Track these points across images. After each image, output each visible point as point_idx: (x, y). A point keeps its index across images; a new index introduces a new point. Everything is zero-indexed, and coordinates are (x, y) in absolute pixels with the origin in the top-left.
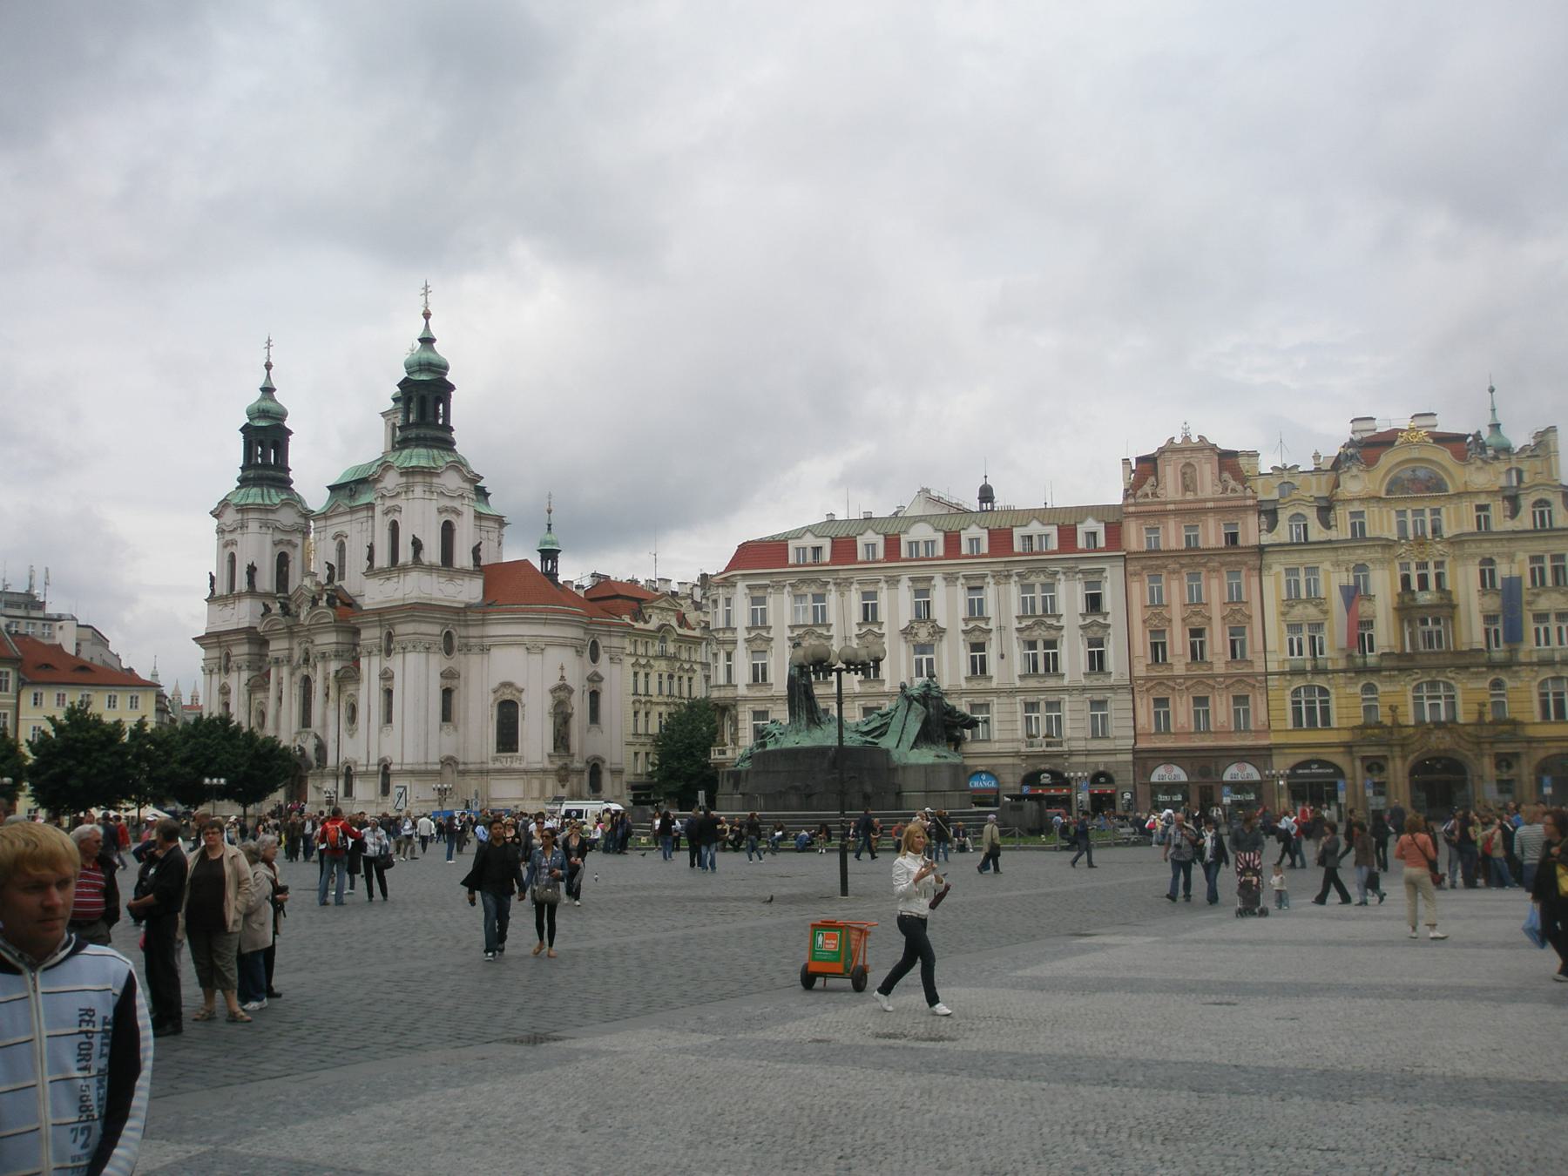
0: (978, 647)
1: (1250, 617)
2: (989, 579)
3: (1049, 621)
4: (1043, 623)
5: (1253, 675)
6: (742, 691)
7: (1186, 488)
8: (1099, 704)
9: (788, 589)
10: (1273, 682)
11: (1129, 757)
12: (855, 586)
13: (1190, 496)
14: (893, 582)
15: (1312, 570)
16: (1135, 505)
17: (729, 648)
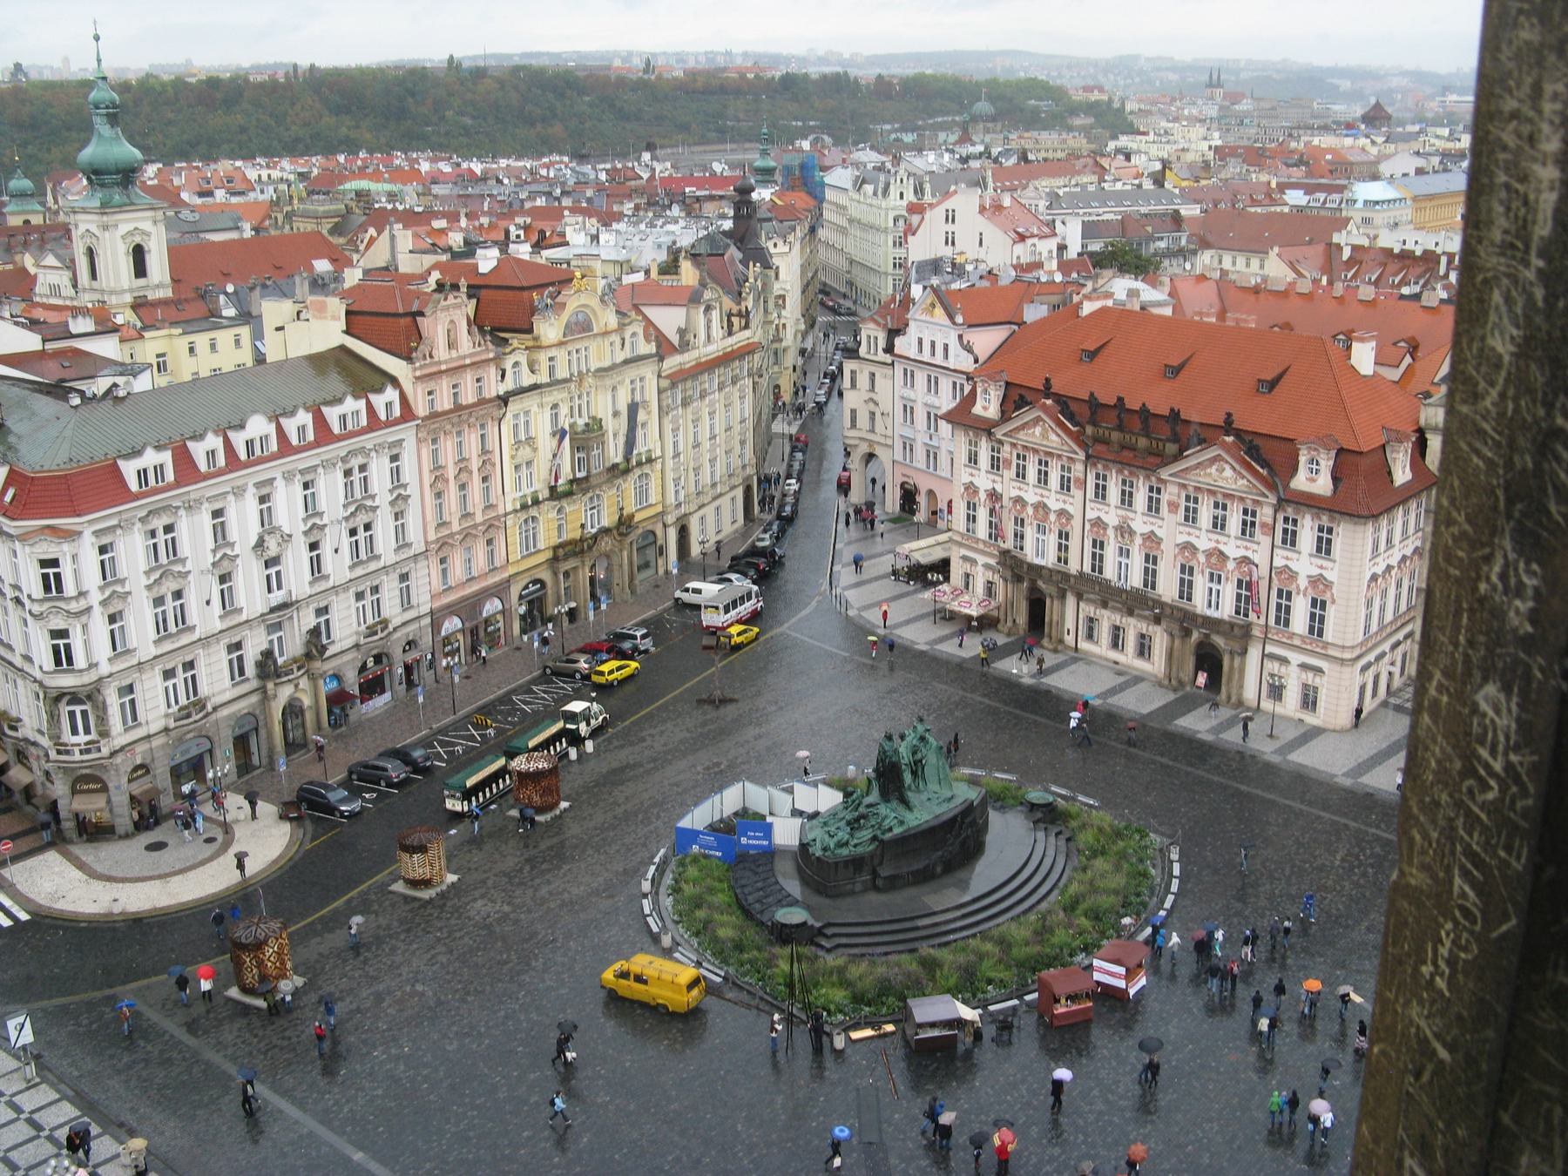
0: (314, 546)
1: (494, 465)
2: (320, 470)
3: (369, 503)
4: (365, 507)
5: (497, 518)
6: (105, 669)
7: (451, 345)
8: (404, 577)
9: (139, 525)
10: (510, 521)
11: (428, 620)
12: (206, 505)
13: (454, 354)
14: (239, 492)
15: (527, 413)
16: (421, 367)
17: (84, 619)
